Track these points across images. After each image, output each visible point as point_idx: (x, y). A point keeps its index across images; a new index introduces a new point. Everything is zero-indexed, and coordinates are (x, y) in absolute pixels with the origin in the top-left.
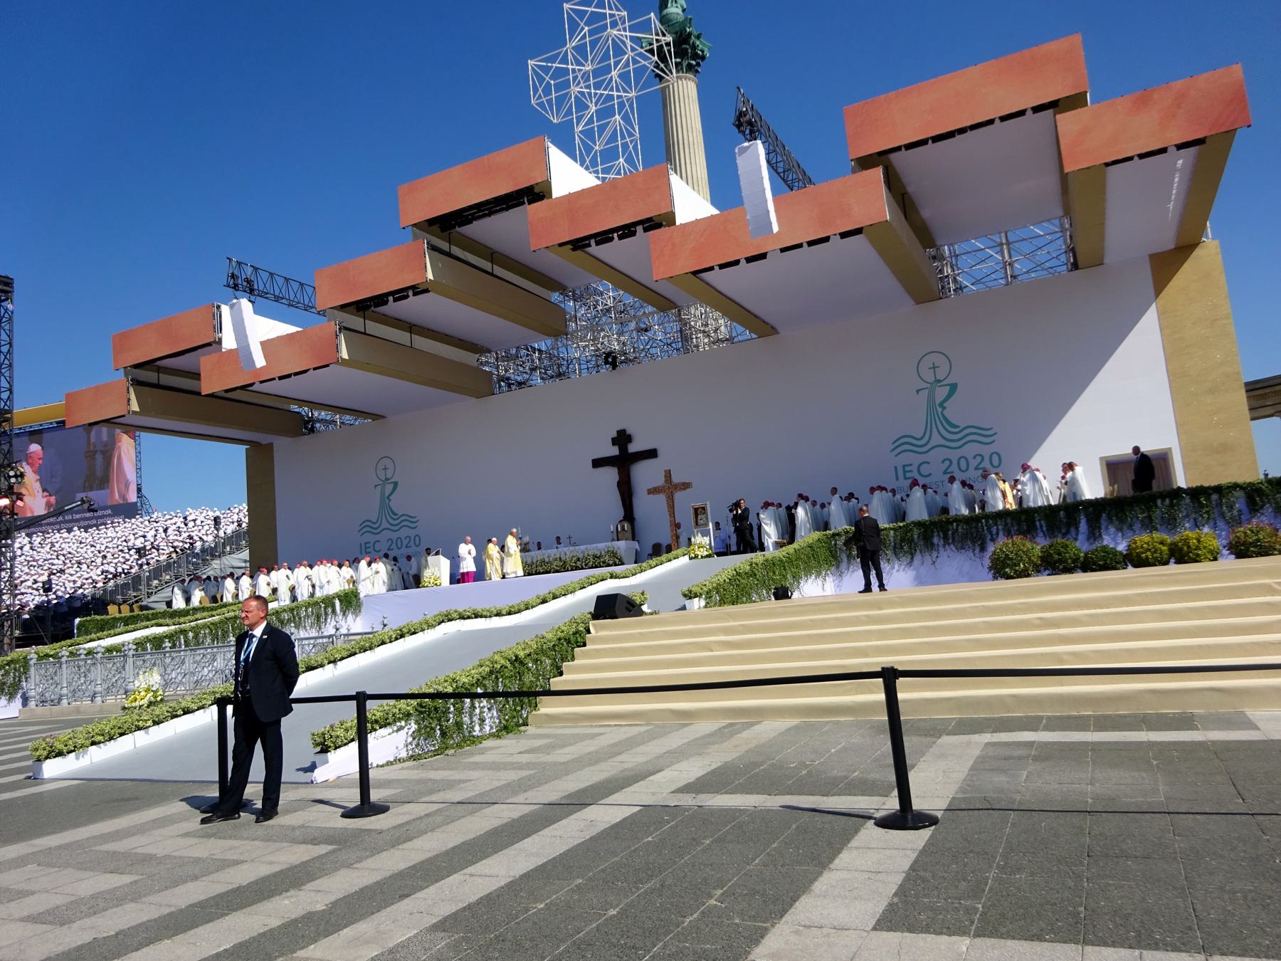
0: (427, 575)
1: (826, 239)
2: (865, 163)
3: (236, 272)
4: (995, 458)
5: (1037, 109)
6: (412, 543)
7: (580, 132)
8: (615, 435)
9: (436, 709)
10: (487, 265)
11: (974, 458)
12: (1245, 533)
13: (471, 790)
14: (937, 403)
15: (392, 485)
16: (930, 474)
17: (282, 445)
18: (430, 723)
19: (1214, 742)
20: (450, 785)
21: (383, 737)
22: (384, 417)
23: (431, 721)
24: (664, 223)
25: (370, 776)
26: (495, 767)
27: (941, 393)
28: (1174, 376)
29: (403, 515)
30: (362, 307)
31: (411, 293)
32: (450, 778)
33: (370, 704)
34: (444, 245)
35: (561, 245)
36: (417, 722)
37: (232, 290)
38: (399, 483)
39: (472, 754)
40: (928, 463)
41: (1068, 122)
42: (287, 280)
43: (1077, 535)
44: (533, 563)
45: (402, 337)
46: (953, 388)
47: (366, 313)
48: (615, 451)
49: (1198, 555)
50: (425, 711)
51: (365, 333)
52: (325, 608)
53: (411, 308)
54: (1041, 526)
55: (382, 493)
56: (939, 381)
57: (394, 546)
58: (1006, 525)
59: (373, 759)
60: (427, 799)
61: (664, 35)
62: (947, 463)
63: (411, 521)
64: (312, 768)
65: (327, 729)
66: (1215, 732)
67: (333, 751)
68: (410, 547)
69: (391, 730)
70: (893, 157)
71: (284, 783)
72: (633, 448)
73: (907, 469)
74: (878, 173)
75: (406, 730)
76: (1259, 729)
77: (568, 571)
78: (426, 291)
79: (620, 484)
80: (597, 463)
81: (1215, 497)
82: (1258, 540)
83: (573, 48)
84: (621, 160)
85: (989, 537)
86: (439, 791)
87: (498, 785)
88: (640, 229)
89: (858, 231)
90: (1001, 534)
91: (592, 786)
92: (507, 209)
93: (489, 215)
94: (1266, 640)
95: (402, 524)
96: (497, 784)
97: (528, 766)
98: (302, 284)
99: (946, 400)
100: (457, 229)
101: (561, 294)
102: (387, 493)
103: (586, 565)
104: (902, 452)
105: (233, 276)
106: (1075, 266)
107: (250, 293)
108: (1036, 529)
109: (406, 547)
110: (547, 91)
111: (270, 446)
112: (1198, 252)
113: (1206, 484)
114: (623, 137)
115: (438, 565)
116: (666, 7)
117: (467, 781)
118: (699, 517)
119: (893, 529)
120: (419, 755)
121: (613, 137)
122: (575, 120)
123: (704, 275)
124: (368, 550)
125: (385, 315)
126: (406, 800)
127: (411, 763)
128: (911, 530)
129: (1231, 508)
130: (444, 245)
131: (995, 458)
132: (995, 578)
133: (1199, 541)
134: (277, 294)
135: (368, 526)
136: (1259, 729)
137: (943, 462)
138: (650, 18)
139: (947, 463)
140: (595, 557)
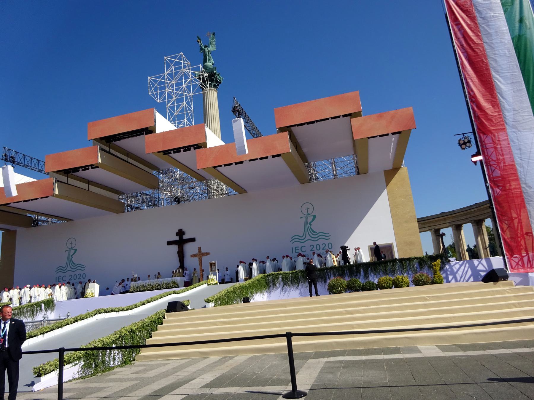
0: (88, 292)
1: (267, 158)
2: (282, 130)
3: (7, 154)
4: (330, 244)
5: (344, 116)
6: (81, 277)
7: (169, 107)
8: (177, 231)
9: (93, 355)
10: (125, 158)
11: (322, 245)
12: (418, 276)
13: (110, 392)
14: (308, 223)
15: (74, 250)
16: (305, 251)
17: (21, 231)
18: (90, 361)
19: (406, 358)
20: (100, 389)
21: (68, 368)
22: (72, 220)
23: (91, 360)
24: (202, 146)
25: (63, 388)
26: (120, 380)
27: (310, 219)
28: (394, 216)
29: (78, 264)
30: (67, 172)
31: (90, 168)
32: (99, 387)
33: (65, 353)
34: (107, 149)
35: (159, 152)
36: (84, 361)
37: (4, 161)
38: (77, 250)
39: (110, 375)
40: (305, 246)
41: (355, 121)
42: (31, 158)
43: (360, 276)
44: (138, 286)
45: (84, 186)
46: (314, 217)
47: (68, 175)
48: (177, 238)
49: (402, 285)
50: (88, 356)
51: (67, 184)
52: (37, 307)
53: (90, 174)
54: (347, 273)
55: (69, 254)
56: (309, 214)
57: (73, 278)
58: (334, 272)
59: (65, 379)
60: (89, 396)
61: (205, 73)
62: (312, 247)
63: (82, 267)
64: (32, 384)
65: (41, 366)
66: (407, 354)
67: (43, 376)
68: (80, 279)
69: (71, 365)
70: (292, 128)
71: (18, 392)
72: (185, 237)
73: (297, 249)
74: (287, 134)
75: (79, 365)
76: (422, 353)
77: (154, 290)
78: (98, 167)
79: (178, 252)
80: (169, 243)
81: (408, 262)
82: (422, 279)
83: (168, 74)
84: (185, 119)
85: (328, 277)
86: (95, 392)
87: (122, 389)
88: (192, 148)
89: (279, 155)
90: (332, 276)
91: (165, 387)
92: (136, 136)
93: (128, 138)
94: (424, 318)
95: (78, 268)
96: (122, 388)
97: (136, 379)
98: (38, 161)
99: (312, 221)
100: (113, 142)
101: (157, 171)
102: (71, 254)
103: (162, 288)
104: (294, 242)
105: (5, 155)
106: (358, 173)
107: (13, 163)
108: (345, 274)
109: (79, 279)
110: (156, 90)
111: (15, 232)
112: (400, 171)
113: (405, 258)
114: (186, 110)
115: (94, 287)
116: (206, 62)
117: (107, 387)
118: (212, 267)
119: (291, 273)
120: (84, 376)
121: (182, 110)
122: (167, 102)
123: (218, 168)
124: (59, 280)
125: (77, 176)
126: (79, 397)
127: (80, 380)
128: (298, 274)
129: (413, 266)
130: (107, 149)
131: (330, 245)
132: (330, 294)
133: (402, 279)
134: (26, 164)
135: (60, 269)
136: (422, 353)
137: (310, 246)
138: (200, 66)
139: (312, 247)
140: (166, 284)
